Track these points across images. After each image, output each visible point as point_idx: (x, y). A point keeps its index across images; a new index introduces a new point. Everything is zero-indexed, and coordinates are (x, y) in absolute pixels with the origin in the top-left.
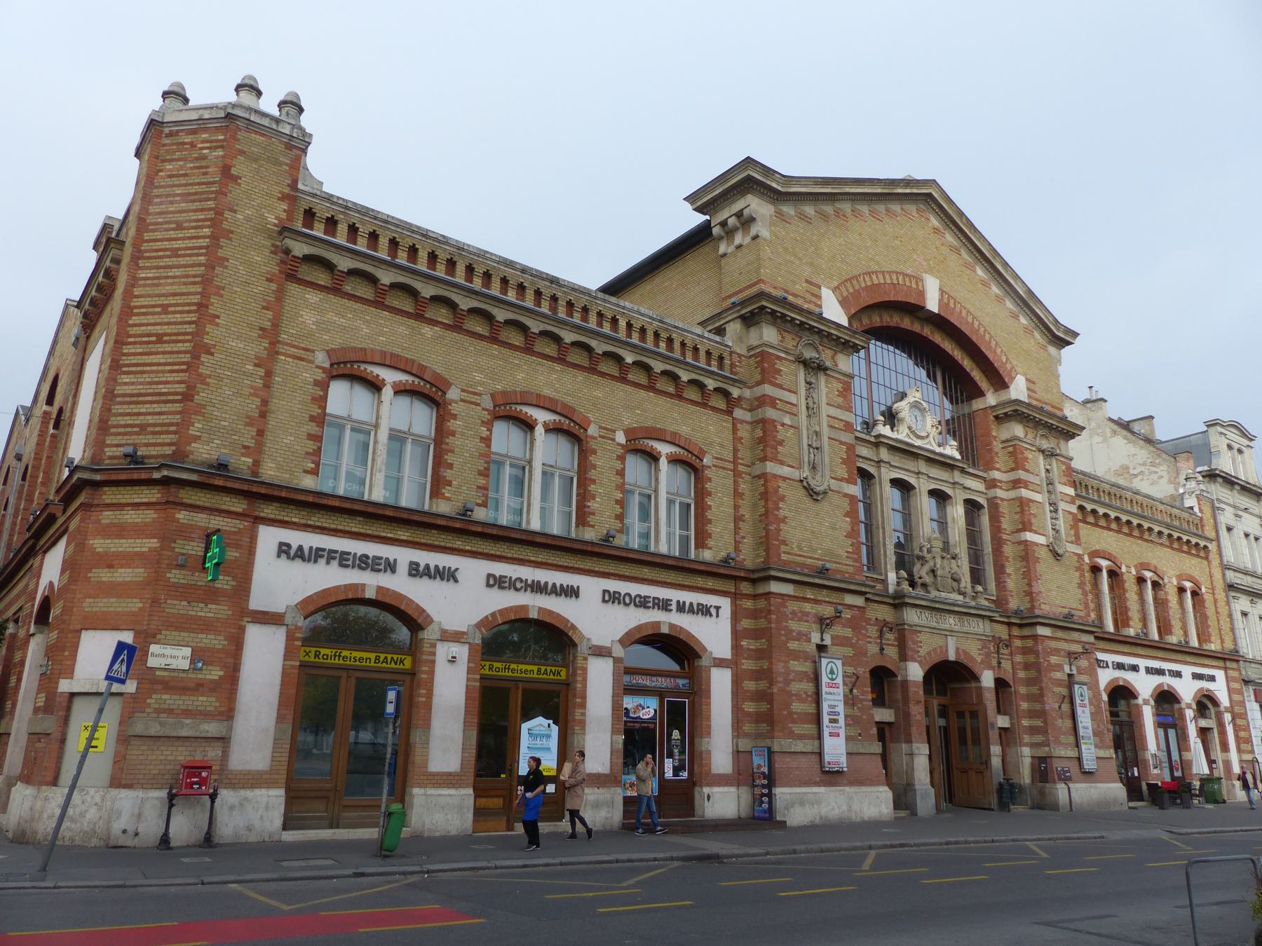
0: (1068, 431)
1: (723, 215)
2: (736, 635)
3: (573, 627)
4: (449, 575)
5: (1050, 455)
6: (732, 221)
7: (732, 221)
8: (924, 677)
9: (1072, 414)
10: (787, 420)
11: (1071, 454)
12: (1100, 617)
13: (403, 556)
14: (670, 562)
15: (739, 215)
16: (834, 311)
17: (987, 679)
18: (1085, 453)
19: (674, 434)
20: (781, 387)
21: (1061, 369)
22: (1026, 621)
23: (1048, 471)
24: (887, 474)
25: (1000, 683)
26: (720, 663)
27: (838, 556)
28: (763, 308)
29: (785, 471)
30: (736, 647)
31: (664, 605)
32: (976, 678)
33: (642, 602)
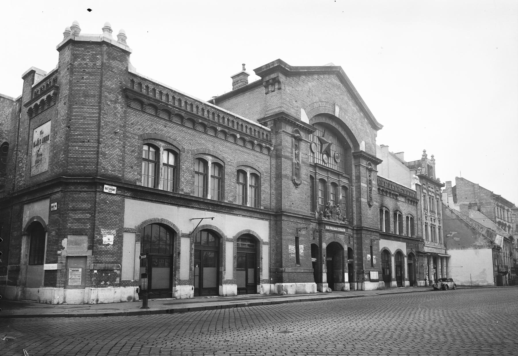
0: (377, 162)
1: (267, 78)
5: (370, 170)
6: (271, 81)
7: (271, 81)
8: (327, 247)
9: (379, 156)
11: (377, 170)
12: (381, 227)
14: (251, 209)
15: (274, 79)
16: (305, 118)
17: (346, 248)
18: (382, 171)
21: (376, 138)
22: (359, 230)
23: (369, 176)
24: (318, 177)
25: (349, 249)
28: (282, 117)
32: (343, 249)
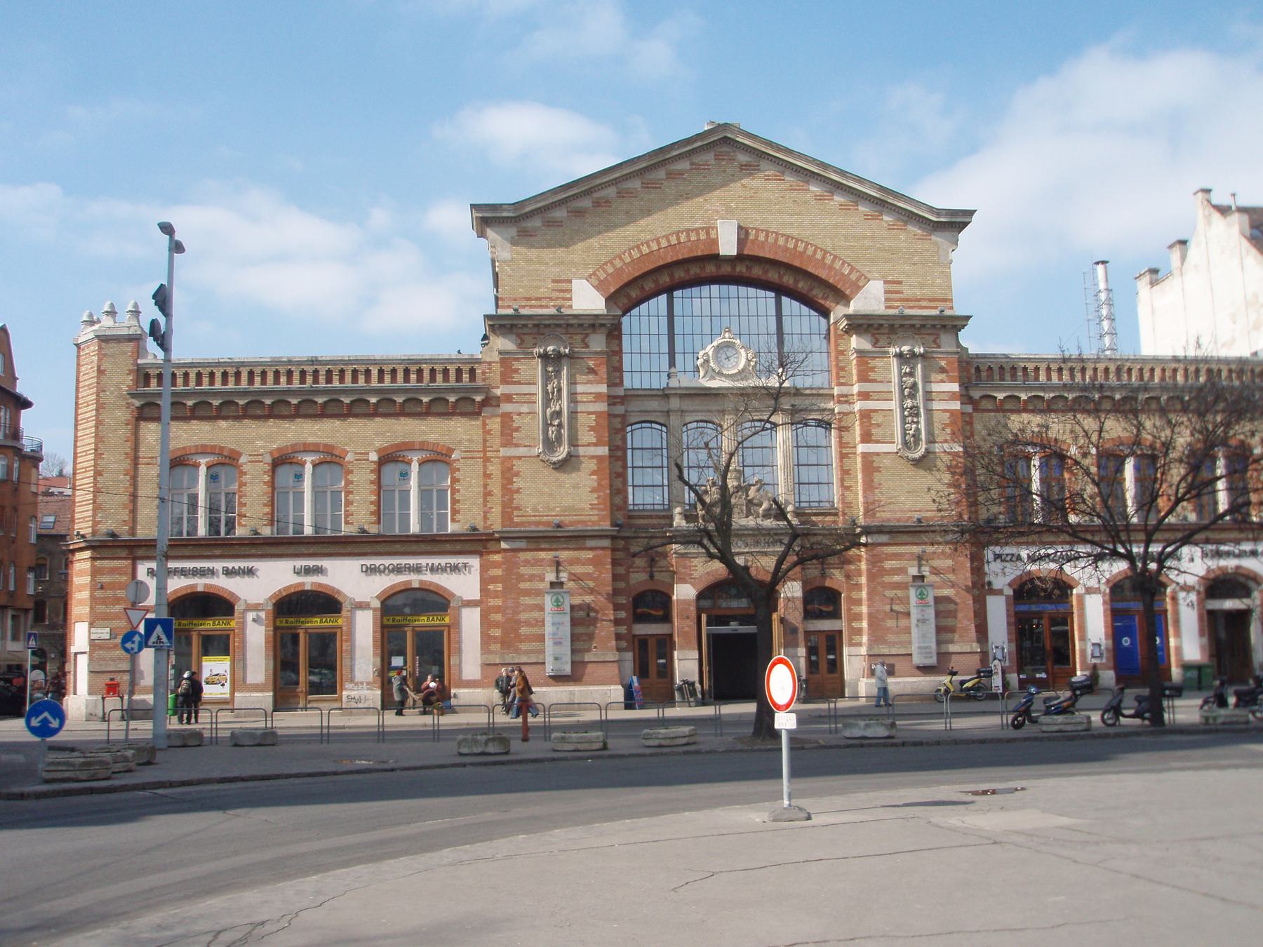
2: (485, 581)
3: (339, 592)
4: (250, 572)
10: (525, 409)
13: (218, 565)
19: (422, 443)
20: (519, 383)
26: (470, 604)
27: (583, 509)
29: (521, 451)
30: (484, 590)
31: (417, 569)
33: (398, 570)
